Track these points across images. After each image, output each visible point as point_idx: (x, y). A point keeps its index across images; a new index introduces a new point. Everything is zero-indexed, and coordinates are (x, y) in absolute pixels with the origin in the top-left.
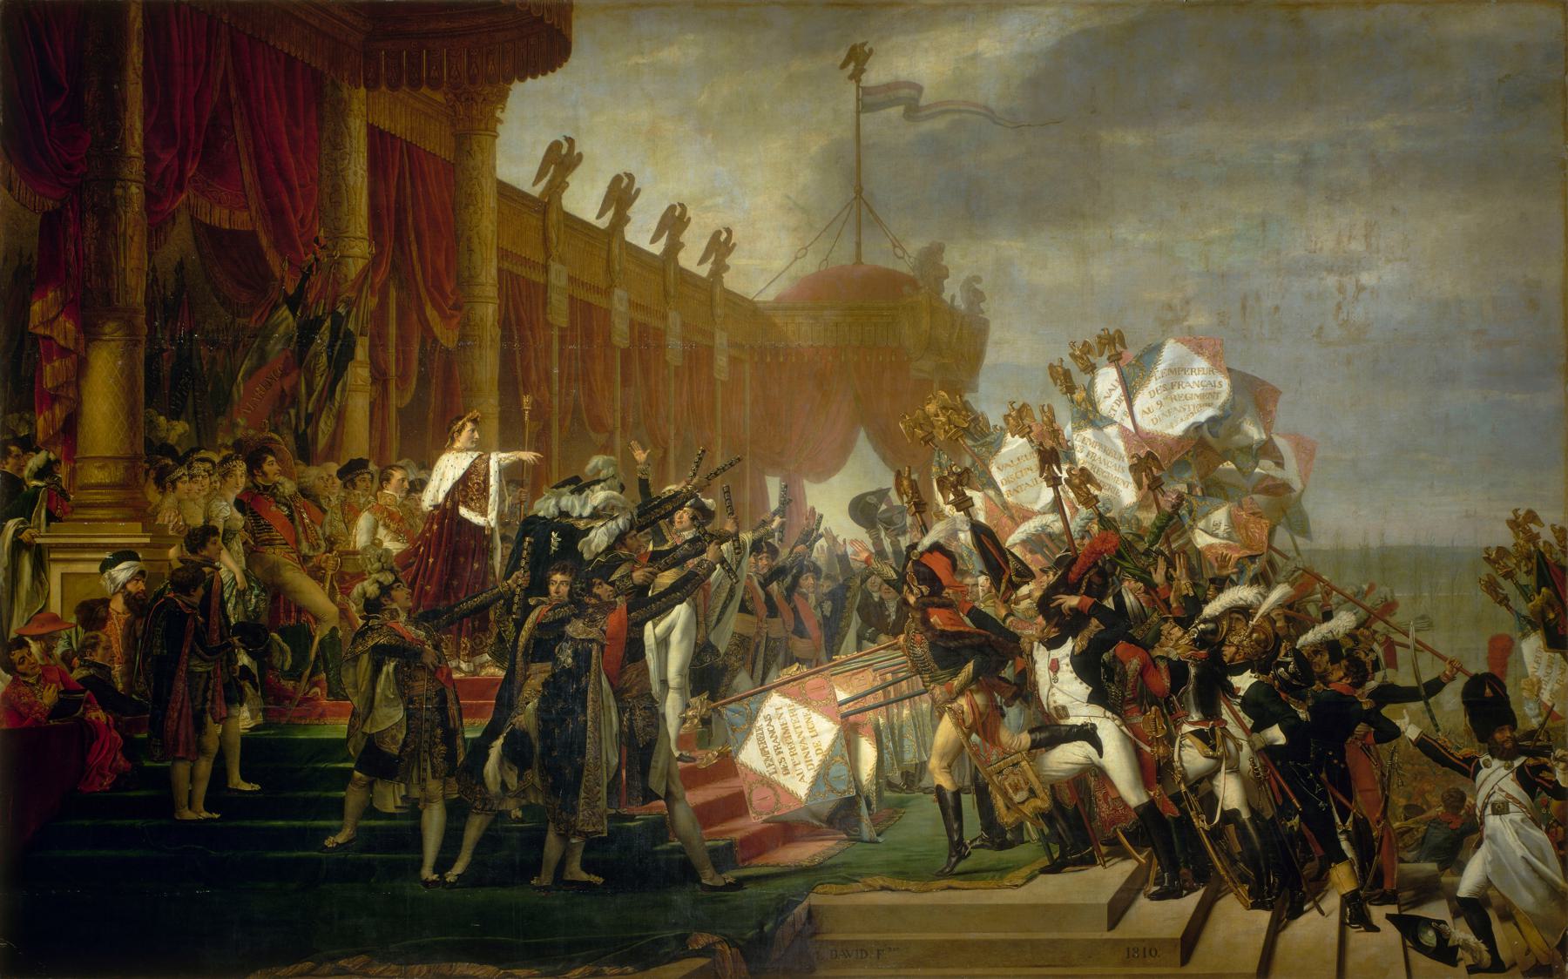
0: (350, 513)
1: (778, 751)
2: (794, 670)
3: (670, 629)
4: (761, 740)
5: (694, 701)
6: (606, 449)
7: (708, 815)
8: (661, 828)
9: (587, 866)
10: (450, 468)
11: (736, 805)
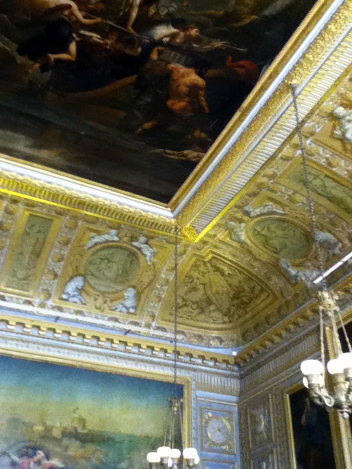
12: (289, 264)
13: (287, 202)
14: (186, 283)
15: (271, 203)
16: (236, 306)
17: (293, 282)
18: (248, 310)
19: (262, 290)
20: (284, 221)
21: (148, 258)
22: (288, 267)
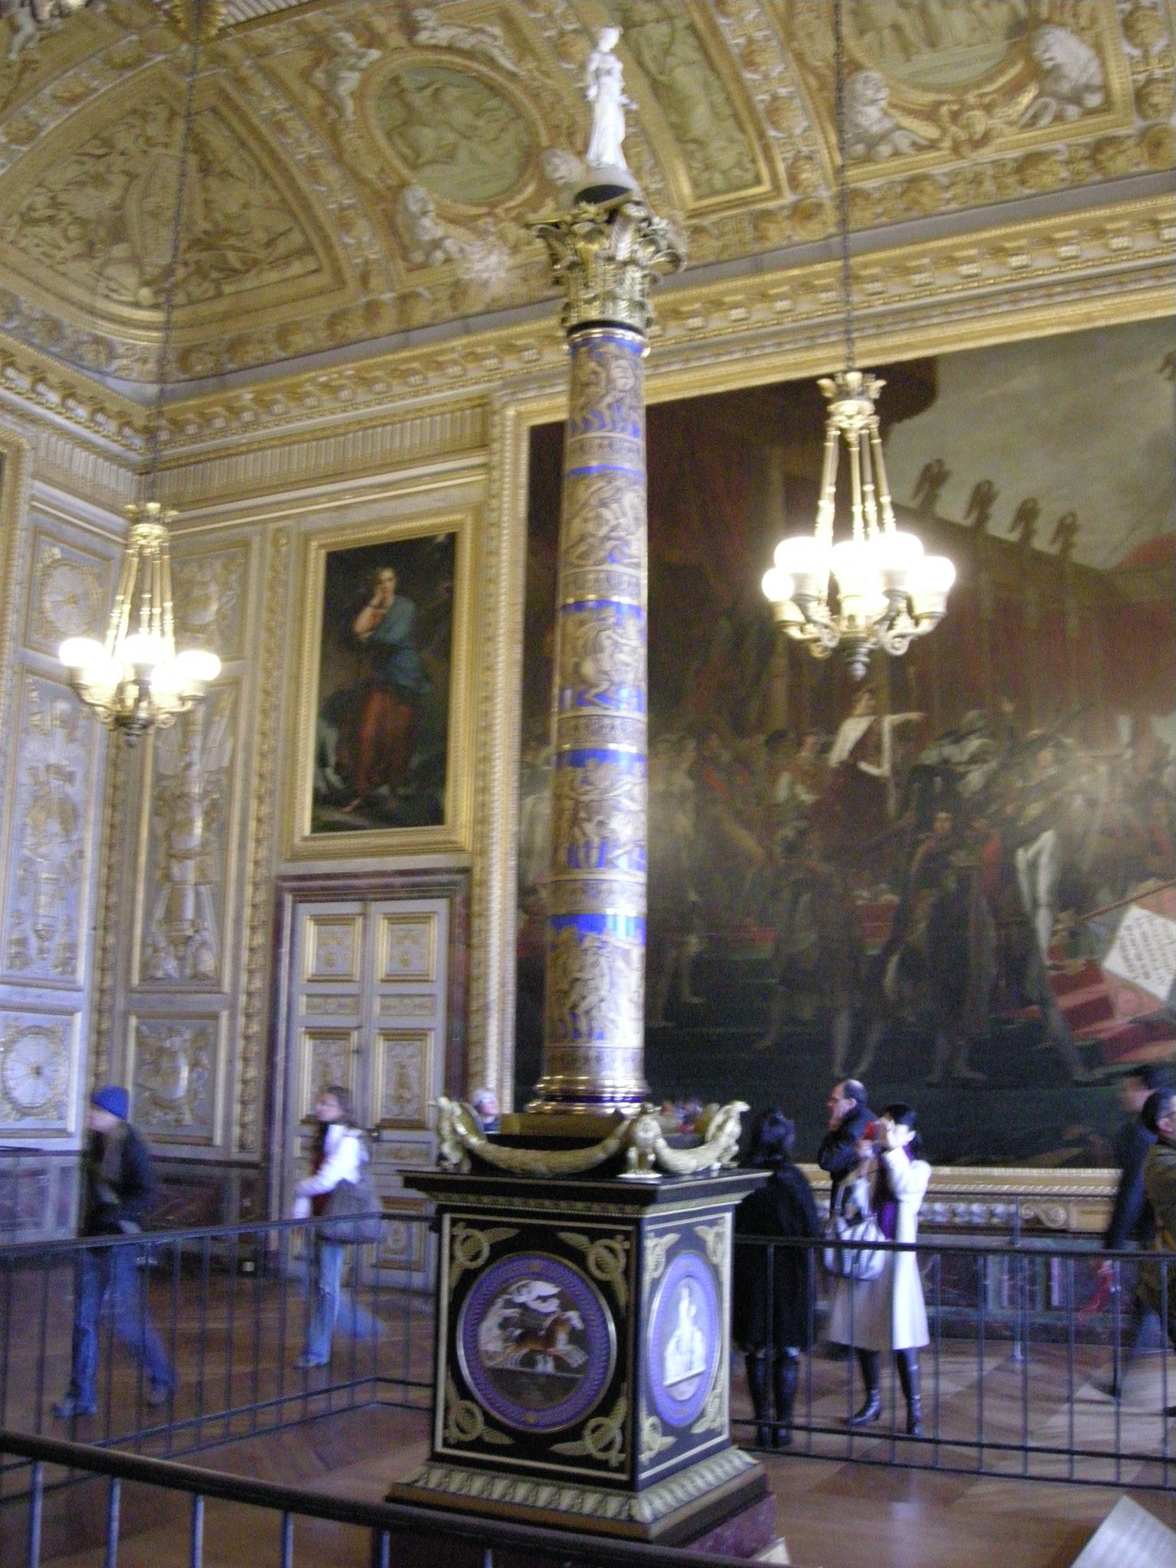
0: (773, 773)
1: (1139, 958)
2: (1151, 884)
3: (1038, 854)
4: (1123, 949)
5: (1063, 916)
6: (978, 704)
7: (1079, 1016)
8: (1038, 1028)
9: (973, 1064)
10: (852, 730)
11: (1103, 1008)
12: (431, 207)
13: (541, 48)
14: (85, 154)
15: (497, 31)
16: (192, 268)
17: (418, 257)
18: (228, 289)
19: (307, 250)
20: (494, 90)
21: (19, 39)
22: (425, 213)
